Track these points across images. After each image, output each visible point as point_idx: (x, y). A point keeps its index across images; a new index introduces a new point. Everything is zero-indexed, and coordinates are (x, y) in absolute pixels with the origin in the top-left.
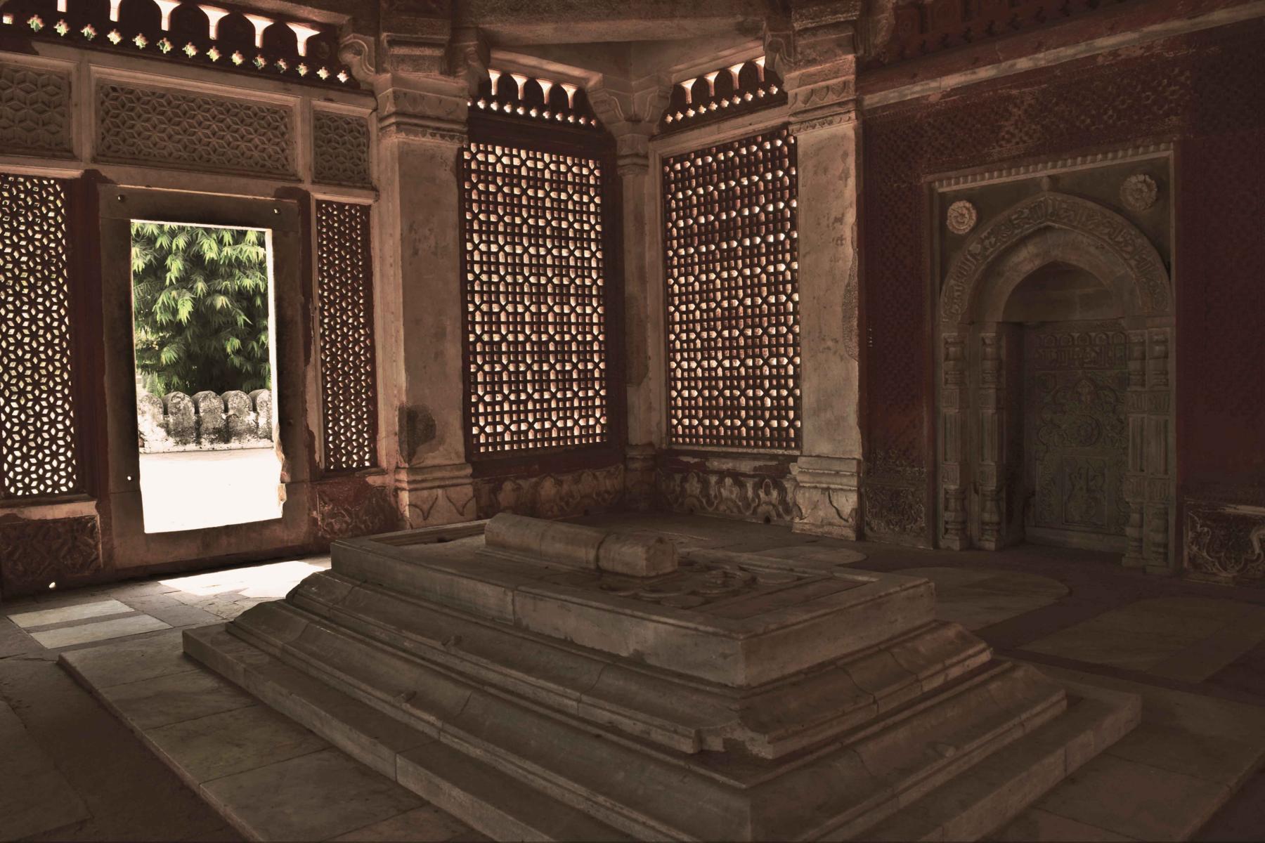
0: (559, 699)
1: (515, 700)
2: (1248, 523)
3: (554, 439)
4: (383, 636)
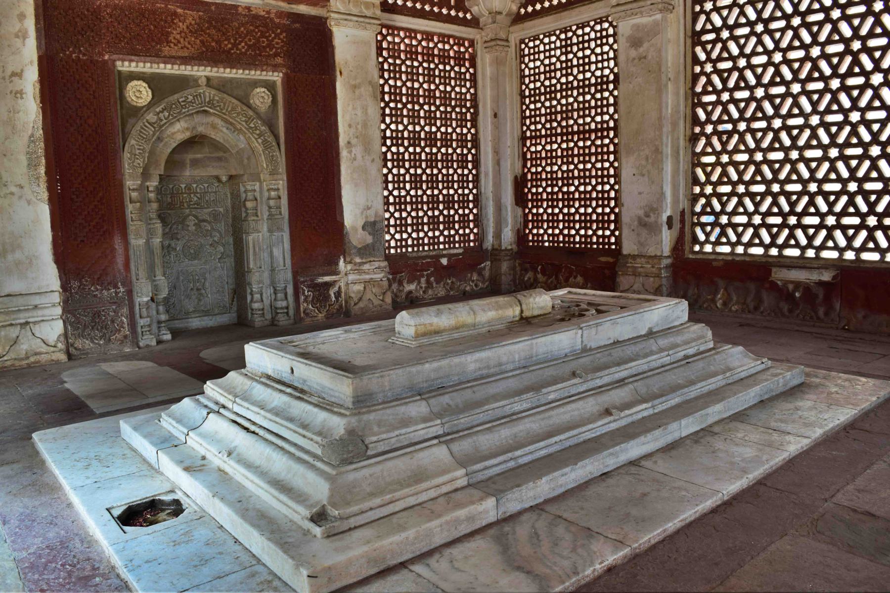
0: (661, 360)
1: (641, 376)
2: (328, 285)
3: (410, 246)
4: (525, 405)
